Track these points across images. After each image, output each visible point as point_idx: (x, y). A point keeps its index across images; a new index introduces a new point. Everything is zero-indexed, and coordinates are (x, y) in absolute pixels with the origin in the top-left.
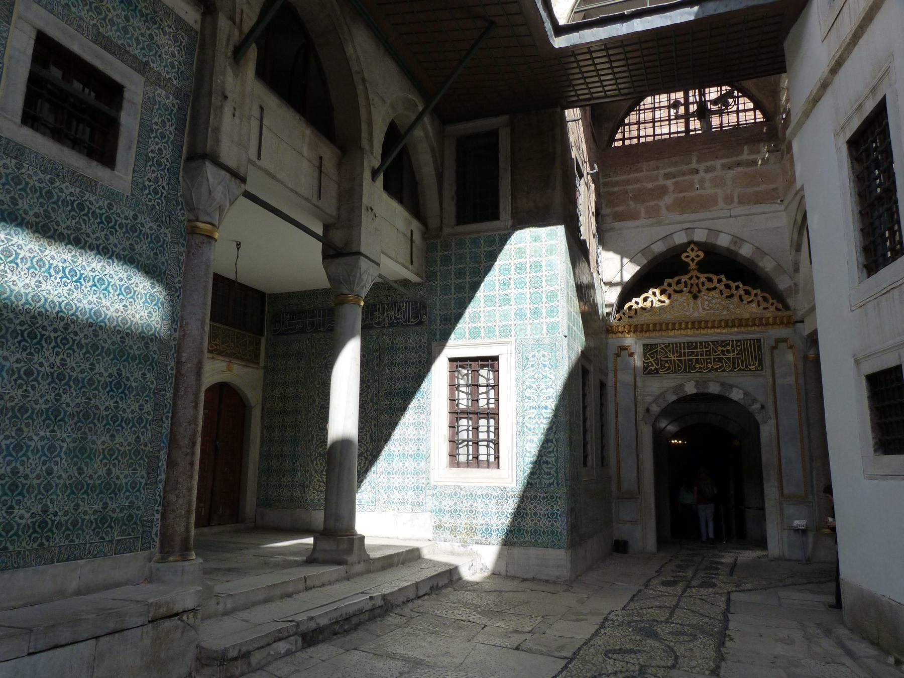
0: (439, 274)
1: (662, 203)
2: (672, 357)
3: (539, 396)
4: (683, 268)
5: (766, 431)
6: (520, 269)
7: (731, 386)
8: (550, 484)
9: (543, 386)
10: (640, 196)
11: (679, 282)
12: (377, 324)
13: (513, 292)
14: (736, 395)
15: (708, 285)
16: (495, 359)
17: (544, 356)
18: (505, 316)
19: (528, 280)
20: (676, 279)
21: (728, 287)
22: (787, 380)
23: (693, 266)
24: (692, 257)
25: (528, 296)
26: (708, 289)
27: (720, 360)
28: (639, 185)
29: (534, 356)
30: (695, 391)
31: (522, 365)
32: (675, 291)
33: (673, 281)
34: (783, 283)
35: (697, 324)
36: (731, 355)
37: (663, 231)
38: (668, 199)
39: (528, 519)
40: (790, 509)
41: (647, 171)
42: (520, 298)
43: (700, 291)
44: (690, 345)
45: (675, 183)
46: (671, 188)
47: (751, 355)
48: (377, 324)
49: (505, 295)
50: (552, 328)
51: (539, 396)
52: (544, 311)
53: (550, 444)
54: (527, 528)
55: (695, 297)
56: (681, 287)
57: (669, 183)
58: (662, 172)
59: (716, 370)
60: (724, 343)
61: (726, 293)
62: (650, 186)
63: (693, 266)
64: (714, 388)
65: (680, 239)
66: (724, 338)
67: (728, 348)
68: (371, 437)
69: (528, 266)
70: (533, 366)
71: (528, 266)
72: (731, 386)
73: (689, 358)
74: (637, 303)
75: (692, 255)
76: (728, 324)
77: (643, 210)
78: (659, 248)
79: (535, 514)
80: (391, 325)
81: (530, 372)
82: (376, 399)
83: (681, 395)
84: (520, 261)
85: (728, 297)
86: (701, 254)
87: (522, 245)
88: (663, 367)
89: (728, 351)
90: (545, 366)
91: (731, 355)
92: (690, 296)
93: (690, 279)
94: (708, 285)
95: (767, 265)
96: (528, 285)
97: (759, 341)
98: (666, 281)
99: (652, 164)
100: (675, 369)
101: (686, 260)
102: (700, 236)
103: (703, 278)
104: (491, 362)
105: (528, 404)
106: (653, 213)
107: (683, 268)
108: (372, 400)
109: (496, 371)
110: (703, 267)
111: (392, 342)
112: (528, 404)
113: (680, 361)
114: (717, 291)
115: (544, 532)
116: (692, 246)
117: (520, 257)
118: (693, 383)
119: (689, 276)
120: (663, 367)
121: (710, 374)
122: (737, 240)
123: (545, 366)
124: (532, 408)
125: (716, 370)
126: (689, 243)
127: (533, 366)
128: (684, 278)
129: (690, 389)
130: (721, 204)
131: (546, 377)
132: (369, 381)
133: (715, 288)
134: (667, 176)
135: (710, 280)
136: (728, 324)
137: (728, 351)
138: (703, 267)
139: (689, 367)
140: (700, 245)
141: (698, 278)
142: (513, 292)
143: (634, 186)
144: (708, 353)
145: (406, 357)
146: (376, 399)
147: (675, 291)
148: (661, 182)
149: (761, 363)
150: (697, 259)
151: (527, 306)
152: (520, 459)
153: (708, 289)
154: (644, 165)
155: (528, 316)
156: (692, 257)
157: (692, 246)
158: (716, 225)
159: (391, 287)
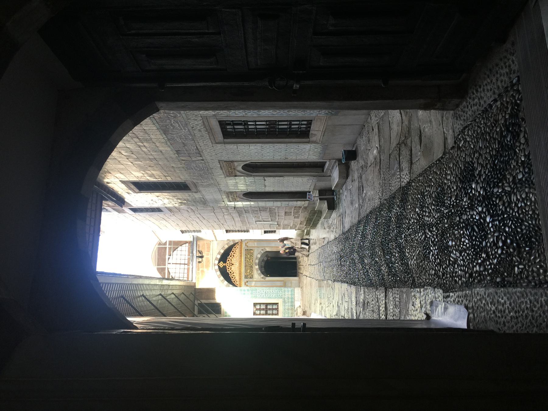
4: (225, 267)
5: (268, 249)
14: (259, 256)
22: (256, 244)
24: (222, 264)
34: (232, 243)
44: (246, 266)
47: (249, 252)
63: (224, 264)
64: (257, 261)
65: (217, 267)
100: (252, 270)
102: (217, 262)
103: (228, 262)
107: (225, 267)
110: (225, 262)
122: (219, 253)
128: (227, 267)
129: (257, 267)
130: (209, 256)
136: (241, 256)
138: (225, 262)
139: (251, 267)
140: (219, 262)
158: (214, 258)
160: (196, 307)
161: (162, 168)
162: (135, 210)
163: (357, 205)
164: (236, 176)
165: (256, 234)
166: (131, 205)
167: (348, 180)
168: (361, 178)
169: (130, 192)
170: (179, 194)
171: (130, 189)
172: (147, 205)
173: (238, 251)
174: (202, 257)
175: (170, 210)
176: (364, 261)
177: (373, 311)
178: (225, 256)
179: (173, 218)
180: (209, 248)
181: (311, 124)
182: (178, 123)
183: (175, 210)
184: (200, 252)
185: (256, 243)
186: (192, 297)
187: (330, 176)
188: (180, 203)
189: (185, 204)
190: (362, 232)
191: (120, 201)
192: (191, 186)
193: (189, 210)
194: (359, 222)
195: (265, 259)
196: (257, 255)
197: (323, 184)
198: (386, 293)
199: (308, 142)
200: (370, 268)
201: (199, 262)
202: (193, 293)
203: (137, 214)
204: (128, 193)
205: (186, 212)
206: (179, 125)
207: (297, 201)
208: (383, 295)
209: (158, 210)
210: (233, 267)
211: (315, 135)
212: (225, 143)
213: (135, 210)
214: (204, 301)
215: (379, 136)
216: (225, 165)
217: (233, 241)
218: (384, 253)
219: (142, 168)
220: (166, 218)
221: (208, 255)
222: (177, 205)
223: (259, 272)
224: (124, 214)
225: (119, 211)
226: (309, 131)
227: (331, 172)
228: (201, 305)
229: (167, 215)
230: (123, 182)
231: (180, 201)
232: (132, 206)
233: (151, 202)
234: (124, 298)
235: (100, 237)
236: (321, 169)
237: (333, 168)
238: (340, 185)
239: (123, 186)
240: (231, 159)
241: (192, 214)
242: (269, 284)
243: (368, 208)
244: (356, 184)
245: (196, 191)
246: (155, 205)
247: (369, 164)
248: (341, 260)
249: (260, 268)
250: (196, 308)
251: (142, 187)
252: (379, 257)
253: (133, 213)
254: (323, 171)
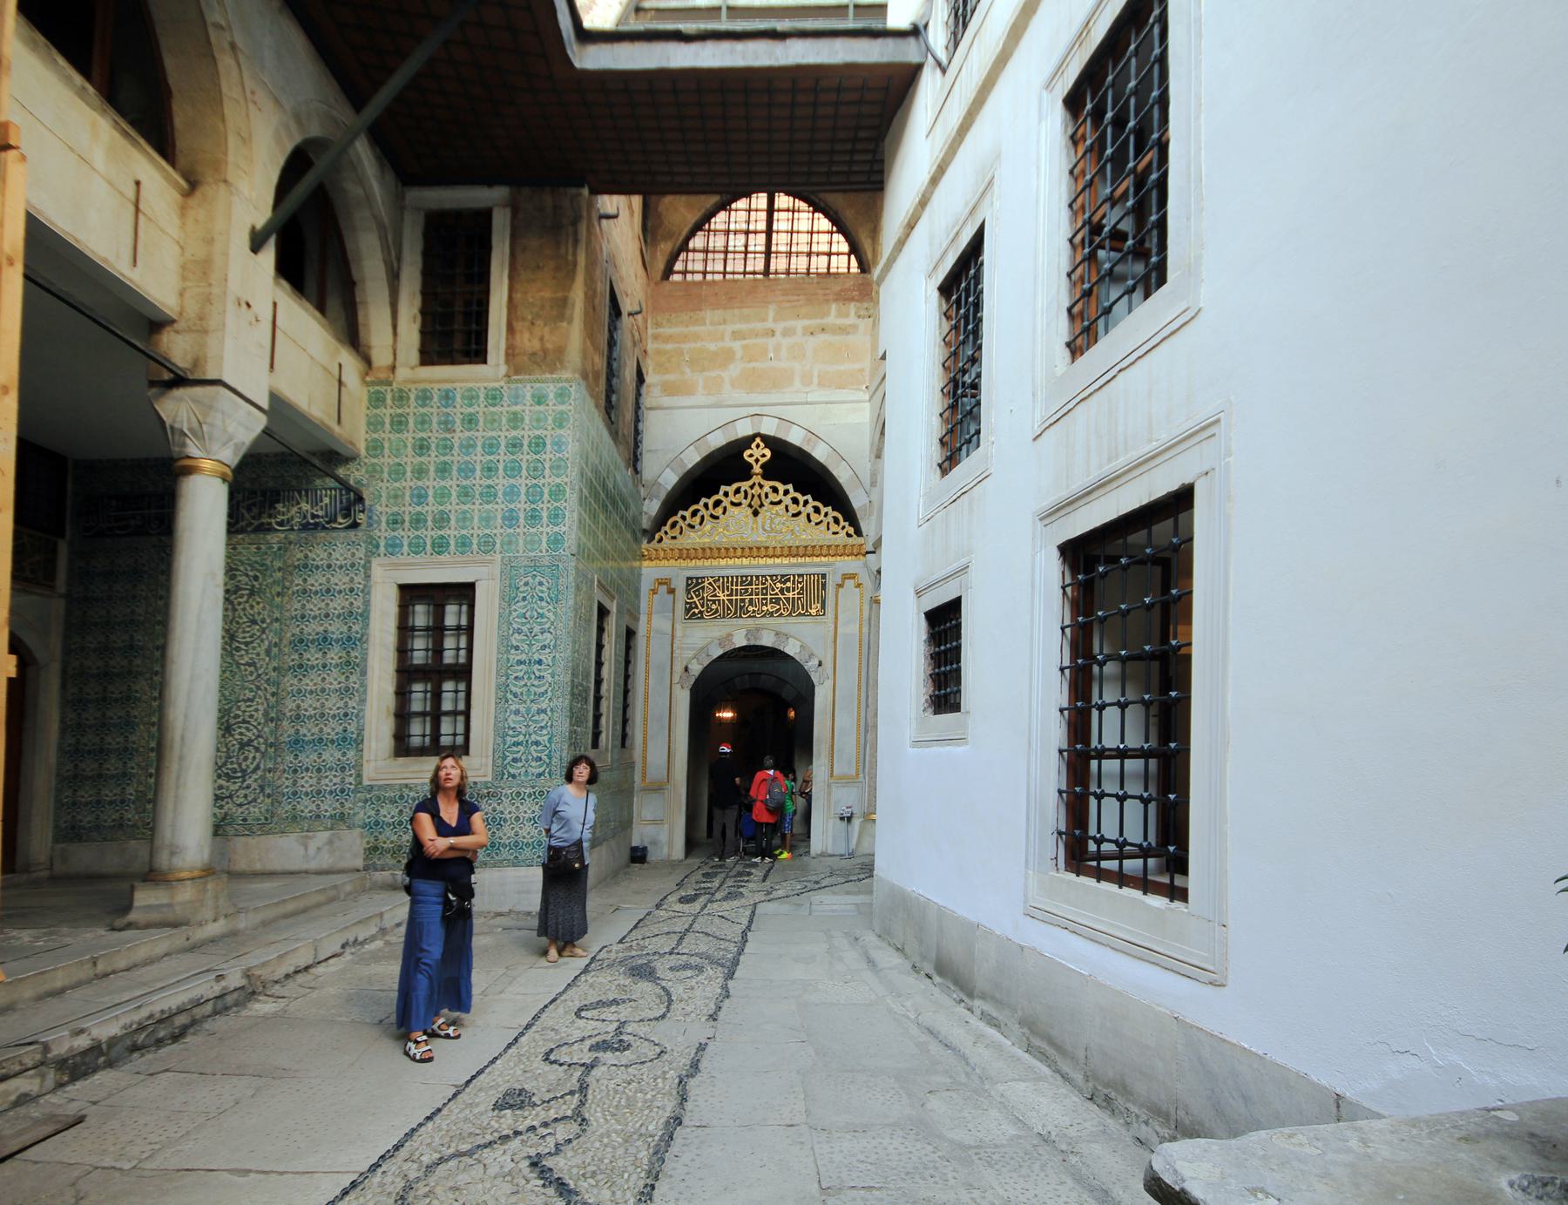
0: (386, 445)
1: (725, 375)
2: (722, 596)
3: (530, 645)
4: (744, 472)
6: (514, 446)
7: (787, 637)
8: (540, 775)
9: (537, 629)
10: (697, 362)
11: (737, 491)
12: (281, 524)
13: (501, 482)
14: (791, 649)
15: (773, 497)
16: (471, 587)
17: (541, 584)
18: (488, 519)
19: (524, 465)
20: (735, 486)
21: (795, 501)
23: (757, 469)
24: (758, 455)
25: (523, 490)
26: (772, 503)
27: (777, 601)
28: (699, 345)
29: (526, 584)
30: (744, 643)
31: (509, 597)
32: (733, 504)
33: (731, 489)
36: (790, 595)
38: (734, 370)
39: (506, 828)
41: (712, 324)
42: (512, 493)
43: (762, 505)
44: (745, 580)
45: (745, 347)
46: (739, 355)
48: (281, 524)
49: (489, 487)
50: (556, 541)
51: (530, 645)
52: (545, 514)
53: (543, 716)
54: (505, 840)
55: (756, 513)
56: (739, 498)
57: (737, 346)
58: (729, 328)
59: (771, 614)
60: (784, 579)
61: (793, 509)
62: (712, 347)
63: (757, 469)
64: (767, 640)
65: (744, 430)
66: (785, 571)
67: (789, 584)
68: (266, 714)
69: (526, 443)
70: (524, 599)
71: (526, 443)
72: (787, 637)
75: (757, 453)
76: (792, 552)
77: (701, 383)
78: (718, 441)
79: (517, 819)
80: (305, 527)
81: (519, 608)
82: (275, 650)
83: (728, 648)
84: (514, 433)
85: (794, 515)
86: (768, 453)
87: (518, 408)
88: (709, 609)
89: (788, 589)
90: (541, 599)
91: (790, 595)
92: (750, 511)
93: (752, 487)
94: (773, 497)
96: (524, 473)
97: (824, 576)
98: (723, 488)
99: (719, 314)
101: (751, 460)
102: (769, 428)
103: (767, 484)
104: (464, 592)
105: (515, 656)
107: (744, 472)
108: (268, 652)
109: (472, 607)
110: (769, 472)
111: (306, 557)
112: (515, 656)
113: (730, 601)
114: (782, 506)
115: (528, 845)
116: (758, 440)
117: (515, 428)
118: (744, 632)
119: (750, 483)
120: (709, 609)
121: (764, 620)
123: (541, 599)
124: (520, 662)
125: (771, 614)
126: (752, 438)
127: (524, 599)
128: (745, 485)
129: (740, 641)
131: (541, 616)
132: (263, 621)
133: (780, 502)
134: (736, 335)
135: (775, 490)
137: (788, 589)
138: (769, 472)
139: (740, 610)
140: (769, 441)
141: (761, 486)
142: (501, 482)
143: (693, 345)
144: (765, 591)
145: (328, 581)
146: (275, 650)
147: (733, 504)
148: (728, 343)
149: (823, 607)
150: (763, 460)
151: (521, 506)
152: (499, 740)
153: (772, 503)
154: (708, 315)
155: (522, 521)
156: (758, 455)
157: (758, 440)
159: (306, 461)
196: (796, 637)
223: (719, 652)
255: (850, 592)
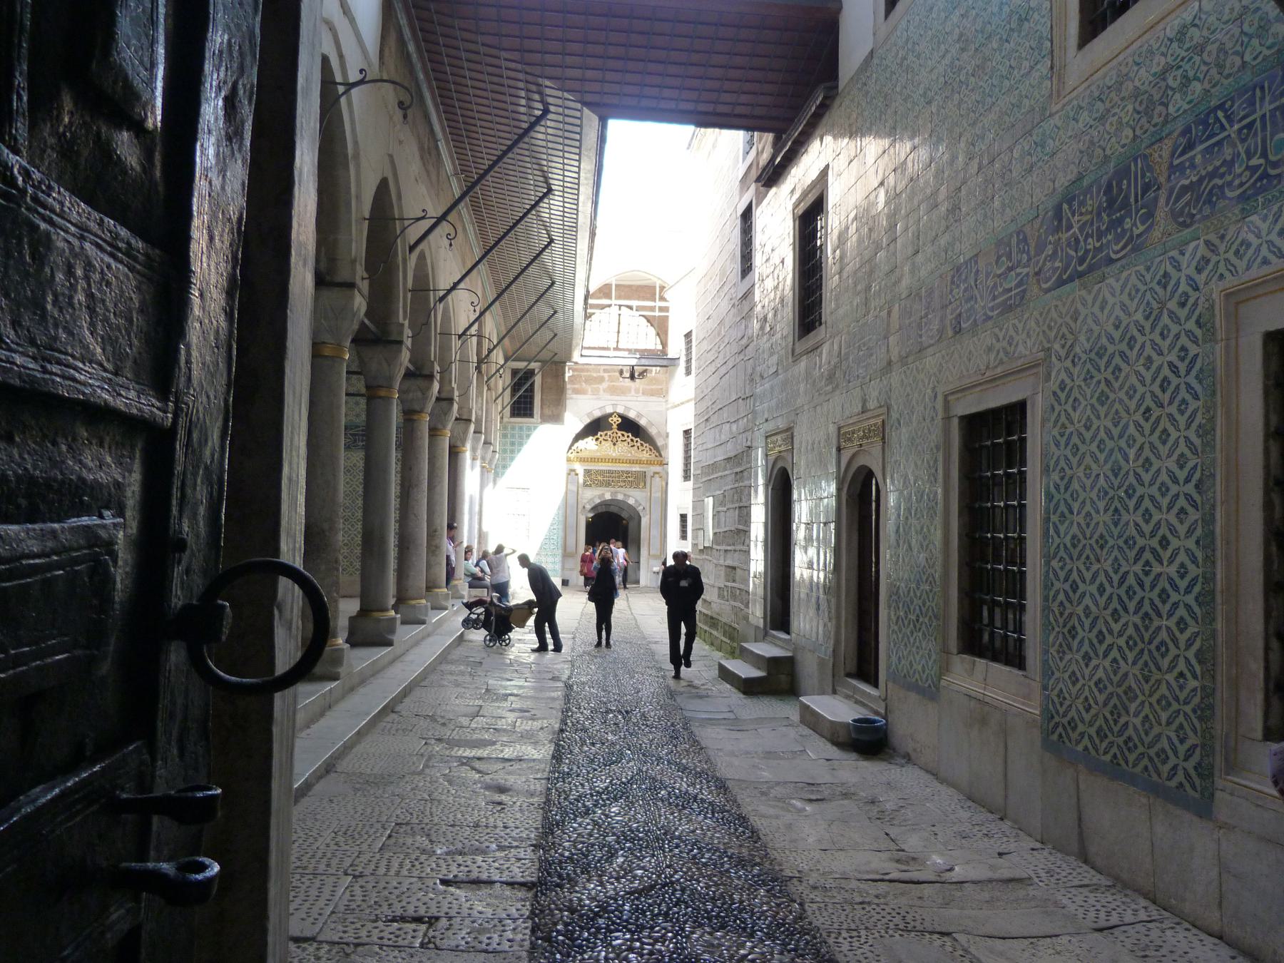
4: (609, 427)
14: (631, 501)
22: (657, 495)
24: (615, 420)
34: (660, 443)
35: (614, 460)
37: (601, 404)
38: (605, 385)
40: (652, 562)
44: (609, 472)
47: (639, 480)
57: (606, 375)
60: (628, 472)
63: (615, 426)
64: (620, 497)
65: (609, 410)
73: (607, 479)
74: (581, 444)
78: (597, 414)
95: (653, 431)
102: (620, 410)
103: (620, 433)
106: (596, 392)
107: (609, 427)
110: (620, 427)
122: (639, 415)
129: (608, 496)
138: (620, 427)
139: (608, 484)
140: (620, 416)
158: (629, 404)
160: (525, 364)
161: (869, 264)
162: (747, 216)
163: (766, 775)
164: (839, 450)
165: (680, 496)
166: (758, 204)
167: (829, 746)
168: (846, 795)
169: (797, 195)
170: (789, 313)
171: (805, 194)
172: (758, 238)
173: (645, 455)
174: (632, 377)
175: (748, 294)
176: (616, 799)
177: (477, 825)
178: (630, 426)
179: (725, 305)
180: (652, 393)
181: (1008, 662)
182: (1017, 286)
183: (746, 309)
184: (642, 374)
185: (659, 495)
186: (546, 355)
187: (834, 692)
188: (765, 319)
189: (762, 328)
190: (695, 798)
191: (771, 176)
192: (812, 339)
193: (744, 341)
194: (722, 786)
195: (624, 515)
196: (634, 497)
197: (809, 668)
198: (523, 884)
199: (945, 651)
200: (595, 823)
201: (621, 372)
202: (556, 358)
203: (739, 221)
204: (792, 192)
205: (740, 335)
206: (1010, 290)
207: (765, 599)
208: (518, 874)
209: (747, 265)
210: (609, 444)
211: (971, 672)
212: (947, 418)
213: (747, 216)
214: (538, 380)
215: (990, 881)
216: (872, 422)
217: (666, 446)
218: (640, 892)
219: (865, 216)
220: (726, 289)
221: (637, 391)
222: (759, 308)
223: (598, 501)
224: (737, 192)
225: (744, 179)
226: (981, 656)
227: (847, 697)
228: (530, 374)
229: (733, 291)
230: (824, 173)
231: (770, 316)
232: (757, 206)
233: (768, 249)
234: (545, 195)
235: (685, 131)
236: (852, 665)
237: (857, 702)
238: (811, 720)
239: (813, 174)
240: (893, 436)
241: (735, 348)
242: (572, 520)
243: (762, 814)
244: (823, 775)
245: (798, 351)
246: (758, 259)
247: (893, 832)
248: (620, 712)
249: (605, 503)
250: (521, 365)
251: (810, 216)
252: (628, 871)
253: (740, 211)
254: (849, 675)
255: (657, 479)
